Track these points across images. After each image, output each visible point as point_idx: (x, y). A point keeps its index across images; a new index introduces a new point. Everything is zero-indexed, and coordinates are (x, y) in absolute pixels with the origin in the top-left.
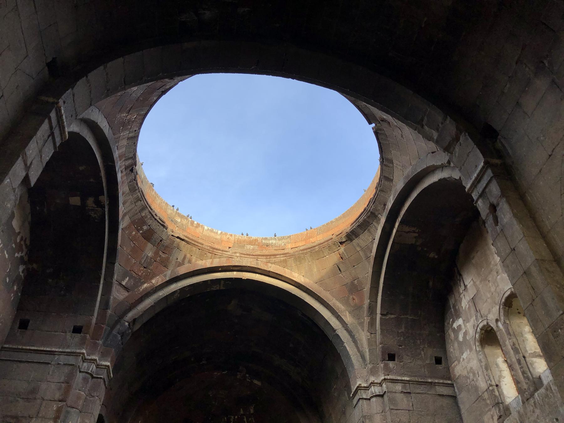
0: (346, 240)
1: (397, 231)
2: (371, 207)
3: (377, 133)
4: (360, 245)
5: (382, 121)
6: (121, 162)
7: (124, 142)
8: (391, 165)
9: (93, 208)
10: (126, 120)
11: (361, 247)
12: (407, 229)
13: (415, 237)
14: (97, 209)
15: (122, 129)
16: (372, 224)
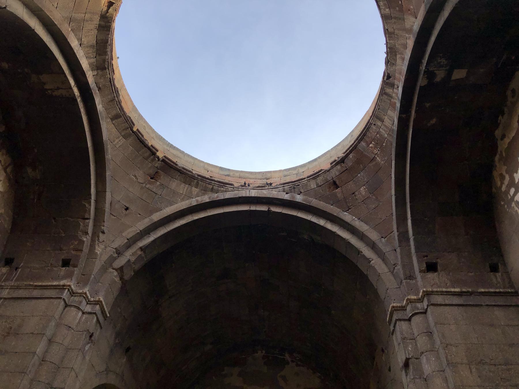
0: (108, 12)
1: (71, 88)
2: (109, 74)
3: (152, 151)
4: (90, 22)
5: (157, 172)
6: (396, 101)
7: (387, 122)
8: (123, 134)
9: (440, 69)
10: (379, 150)
11: (87, 21)
12: (63, 92)
13: (45, 84)
14: (435, 69)
15: (384, 143)
16: (96, 57)
